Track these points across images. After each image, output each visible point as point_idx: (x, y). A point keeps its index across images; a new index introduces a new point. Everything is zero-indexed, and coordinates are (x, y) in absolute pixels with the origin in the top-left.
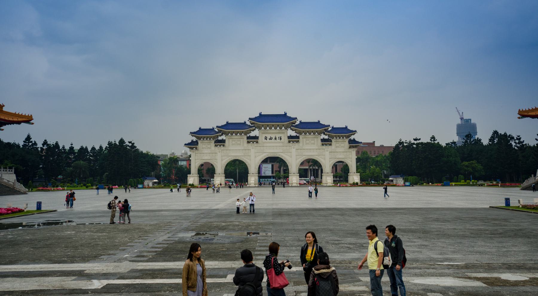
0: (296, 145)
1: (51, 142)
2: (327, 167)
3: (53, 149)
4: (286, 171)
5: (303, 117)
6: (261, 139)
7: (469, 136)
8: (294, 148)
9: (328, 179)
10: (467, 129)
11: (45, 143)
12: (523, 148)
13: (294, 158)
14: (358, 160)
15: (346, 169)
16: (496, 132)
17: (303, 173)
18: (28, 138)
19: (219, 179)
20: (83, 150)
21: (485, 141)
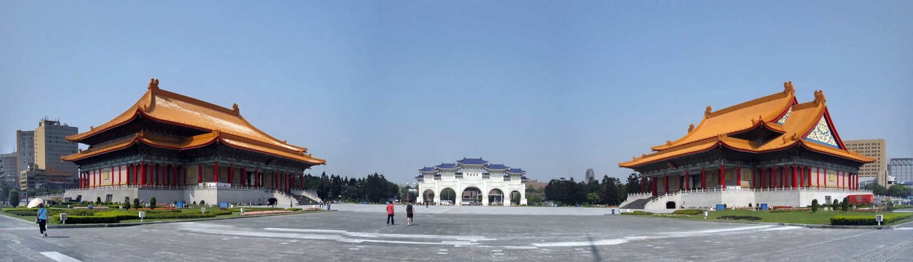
0: (488, 180)
1: (336, 175)
2: (507, 194)
3: (337, 179)
4: (481, 197)
5: (492, 161)
6: (465, 174)
7: (591, 179)
8: (485, 181)
9: (507, 201)
10: (589, 173)
11: (332, 176)
12: (620, 186)
13: (486, 187)
14: (526, 191)
15: (519, 196)
16: (606, 176)
17: (491, 199)
18: (324, 174)
19: (437, 199)
20: (353, 181)
21: (600, 182)
